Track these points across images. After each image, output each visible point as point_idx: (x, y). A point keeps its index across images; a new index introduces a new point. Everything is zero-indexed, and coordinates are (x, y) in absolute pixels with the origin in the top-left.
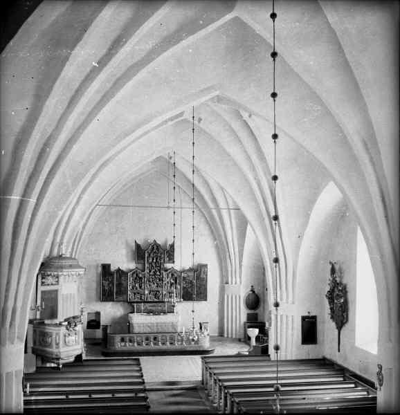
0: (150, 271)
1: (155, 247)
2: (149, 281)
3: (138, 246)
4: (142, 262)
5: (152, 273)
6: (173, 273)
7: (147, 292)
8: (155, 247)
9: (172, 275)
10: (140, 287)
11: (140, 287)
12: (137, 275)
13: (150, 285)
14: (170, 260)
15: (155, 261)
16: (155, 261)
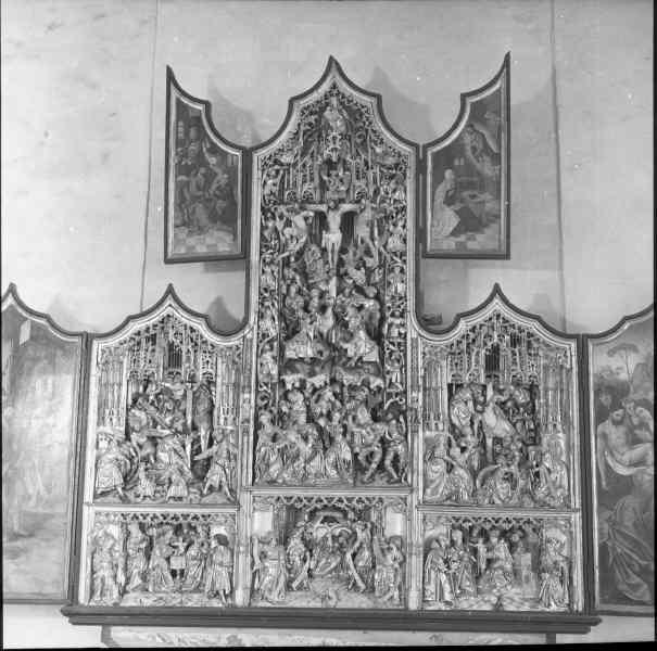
0: (291, 331)
1: (335, 119)
2: (280, 419)
3: (190, 122)
4: (223, 243)
5: (302, 349)
6: (502, 349)
7: (262, 522)
8: (335, 119)
9: (492, 363)
10: (201, 469)
11: (201, 469)
12: (174, 358)
13: (288, 456)
14: (470, 222)
15: (333, 237)
16: (333, 237)
